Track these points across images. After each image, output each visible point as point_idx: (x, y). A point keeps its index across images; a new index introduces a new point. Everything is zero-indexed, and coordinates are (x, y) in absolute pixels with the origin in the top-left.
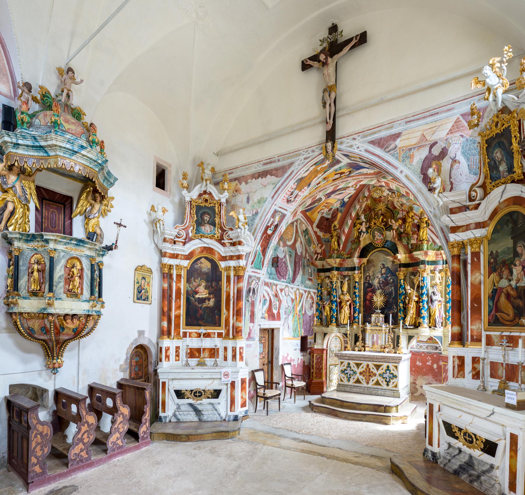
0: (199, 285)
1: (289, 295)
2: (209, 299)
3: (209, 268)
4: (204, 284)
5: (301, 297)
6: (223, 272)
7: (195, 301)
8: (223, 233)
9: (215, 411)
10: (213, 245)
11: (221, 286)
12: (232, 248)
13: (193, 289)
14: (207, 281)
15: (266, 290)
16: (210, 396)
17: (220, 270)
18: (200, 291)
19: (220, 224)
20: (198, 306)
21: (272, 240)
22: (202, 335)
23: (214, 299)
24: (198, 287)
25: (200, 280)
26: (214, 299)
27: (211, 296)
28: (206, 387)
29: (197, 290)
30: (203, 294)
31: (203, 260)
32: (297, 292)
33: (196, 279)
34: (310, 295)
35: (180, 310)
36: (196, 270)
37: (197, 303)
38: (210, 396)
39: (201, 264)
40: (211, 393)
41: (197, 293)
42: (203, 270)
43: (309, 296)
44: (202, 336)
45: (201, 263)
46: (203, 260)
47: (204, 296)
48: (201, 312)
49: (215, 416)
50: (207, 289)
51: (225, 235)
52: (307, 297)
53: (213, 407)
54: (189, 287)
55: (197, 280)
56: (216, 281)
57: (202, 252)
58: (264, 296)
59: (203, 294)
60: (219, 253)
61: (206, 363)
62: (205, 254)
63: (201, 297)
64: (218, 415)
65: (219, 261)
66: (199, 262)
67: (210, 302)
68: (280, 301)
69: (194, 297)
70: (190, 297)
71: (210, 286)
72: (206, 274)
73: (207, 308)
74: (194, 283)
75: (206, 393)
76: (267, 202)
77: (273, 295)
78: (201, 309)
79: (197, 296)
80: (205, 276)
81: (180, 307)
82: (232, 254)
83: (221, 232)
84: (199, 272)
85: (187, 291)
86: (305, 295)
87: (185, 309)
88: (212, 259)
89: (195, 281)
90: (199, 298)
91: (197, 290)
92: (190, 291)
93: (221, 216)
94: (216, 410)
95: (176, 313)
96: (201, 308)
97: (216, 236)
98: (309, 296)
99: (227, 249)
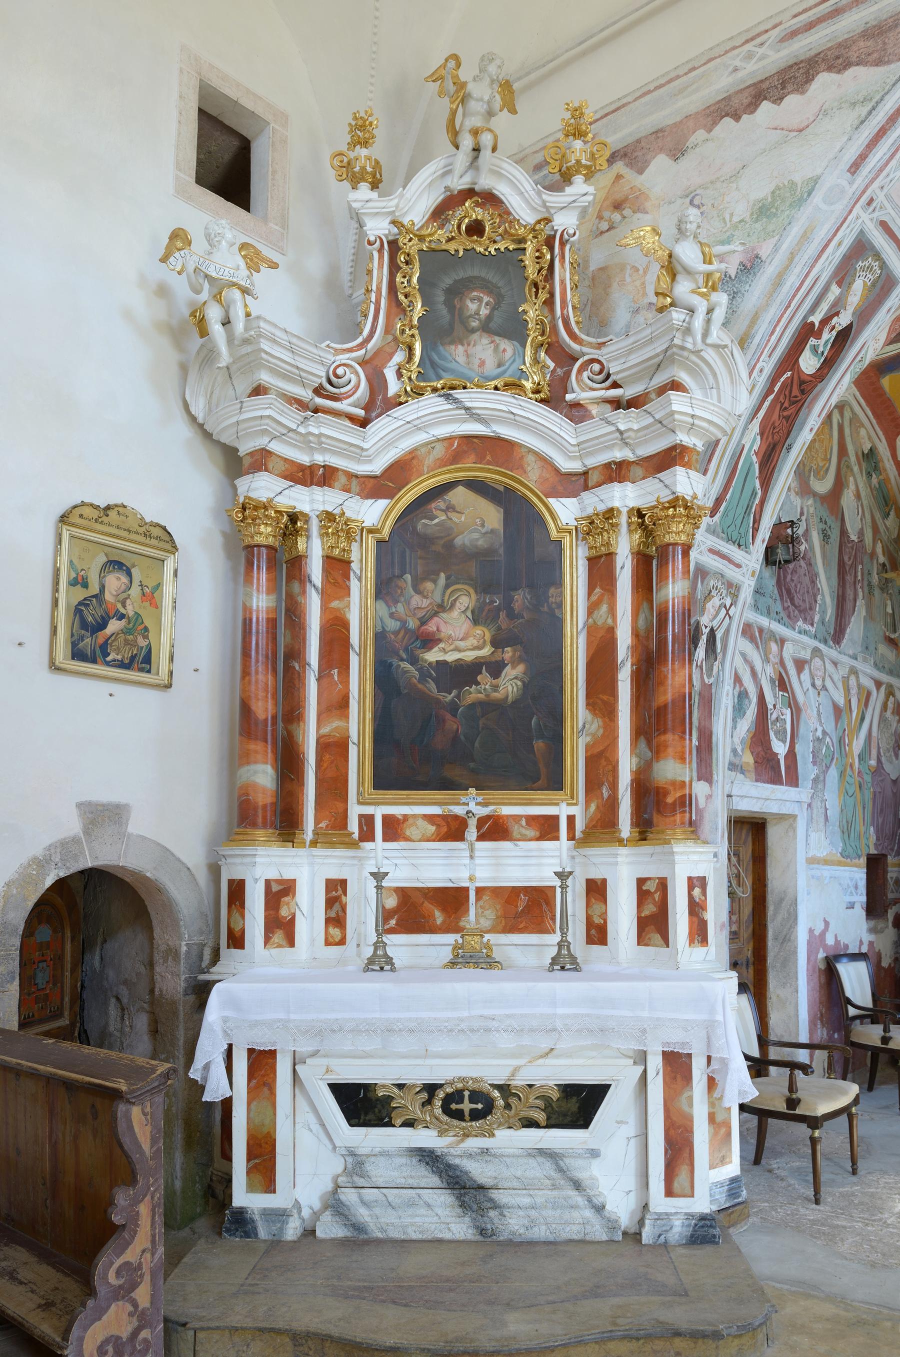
0: (442, 607)
1: (824, 688)
2: (496, 669)
3: (492, 531)
4: (466, 601)
5: (866, 705)
6: (567, 542)
7: (424, 675)
8: (568, 374)
9: (573, 1193)
10: (513, 420)
11: (560, 605)
12: (627, 420)
13: (412, 624)
14: (484, 587)
15: (743, 655)
16: (541, 1117)
17: (554, 534)
18: (446, 631)
19: (548, 331)
20: (438, 701)
21: (810, 409)
22: (472, 823)
23: (521, 668)
24: (436, 614)
25: (447, 586)
26: (521, 668)
27: (508, 653)
28: (517, 1069)
29: (431, 627)
30: (462, 644)
31: (460, 495)
32: (853, 681)
33: (424, 579)
34: (891, 699)
35: (347, 717)
36: (425, 541)
37: (432, 686)
38: (541, 1117)
39: (454, 516)
40: (546, 1099)
41: (429, 641)
42: (458, 541)
43: (890, 705)
44: (472, 833)
45: (450, 508)
46: (460, 495)
47: (469, 656)
48: (452, 724)
49: (575, 1214)
50: (485, 624)
51: (580, 372)
52: (885, 707)
53: (560, 1170)
54: (392, 615)
55: (429, 585)
56: (531, 586)
57: (455, 458)
58: (737, 679)
59: (462, 644)
60: (546, 462)
61: (497, 955)
62: (470, 469)
63: (451, 657)
64: (588, 1213)
65: (548, 496)
66: (440, 504)
67: (500, 681)
68: (796, 709)
69: (414, 660)
70: (395, 662)
71: (498, 609)
72: (482, 556)
73: (488, 706)
74: (417, 600)
75: (513, 1101)
76: (817, 198)
77: (772, 681)
78: (455, 716)
79: (433, 656)
80: (473, 568)
81: (344, 704)
82: (618, 454)
83: (552, 365)
84: (438, 548)
85: (380, 637)
86: (878, 699)
87: (369, 715)
88: (509, 490)
89: (418, 591)
90: (441, 665)
91: (431, 627)
92: (396, 633)
93: (552, 294)
94: (577, 1185)
95: (325, 730)
96: (453, 708)
97: (528, 385)
98: (890, 705)
99: (593, 429)
